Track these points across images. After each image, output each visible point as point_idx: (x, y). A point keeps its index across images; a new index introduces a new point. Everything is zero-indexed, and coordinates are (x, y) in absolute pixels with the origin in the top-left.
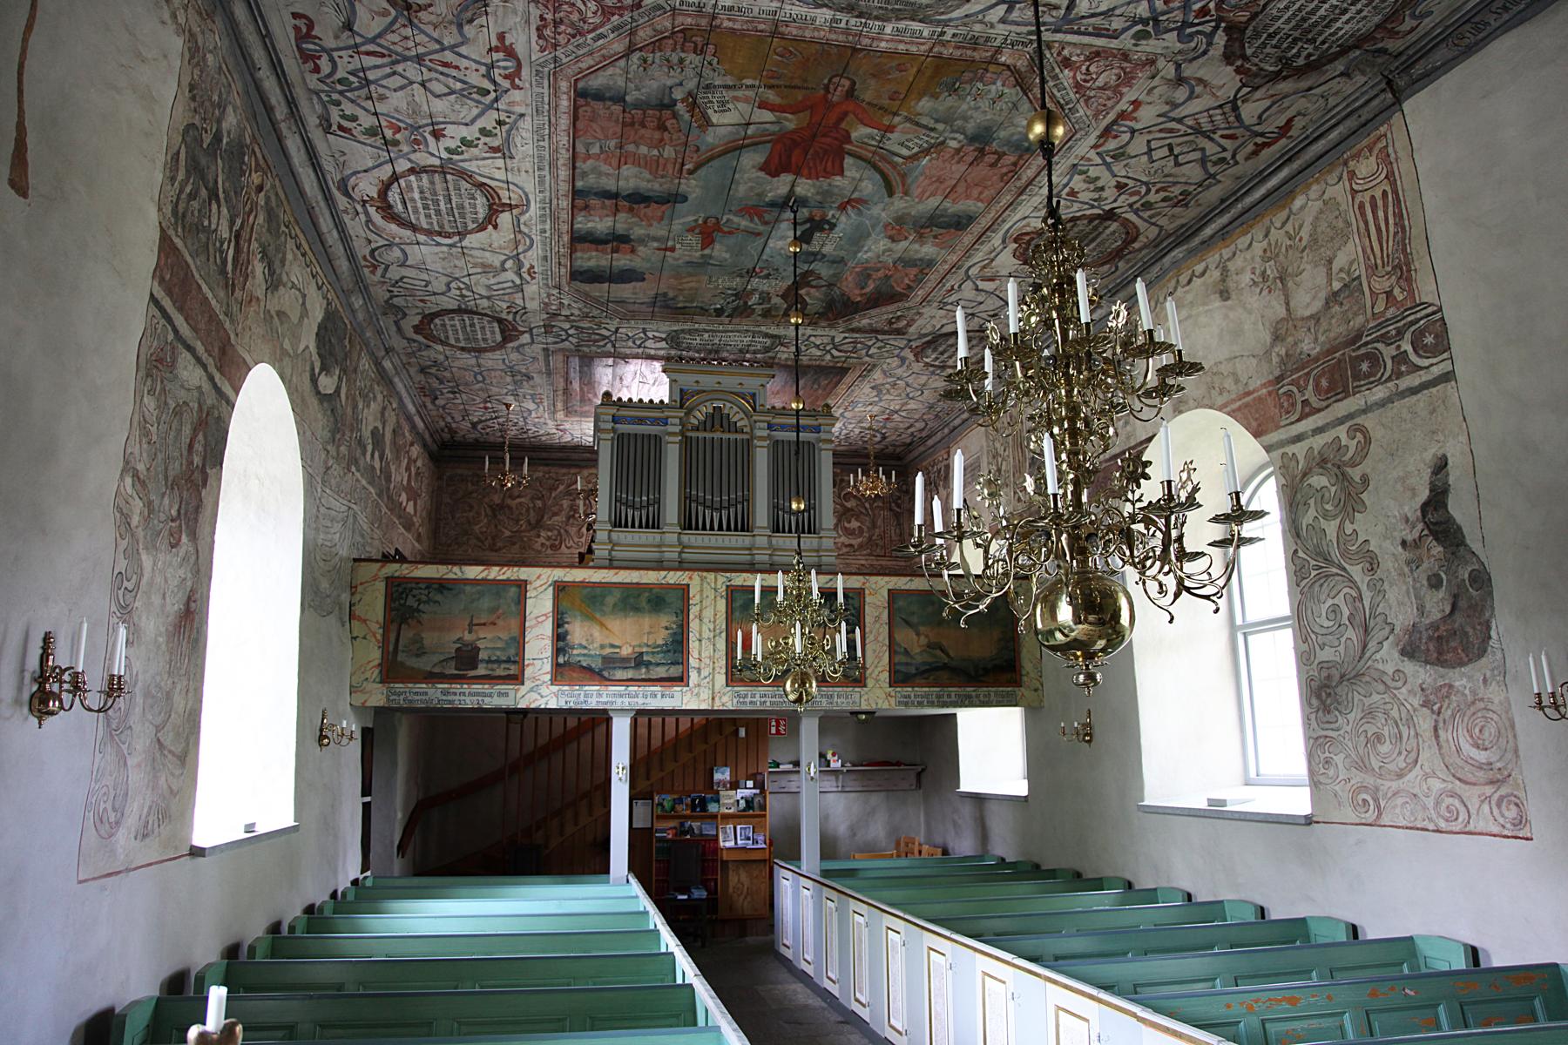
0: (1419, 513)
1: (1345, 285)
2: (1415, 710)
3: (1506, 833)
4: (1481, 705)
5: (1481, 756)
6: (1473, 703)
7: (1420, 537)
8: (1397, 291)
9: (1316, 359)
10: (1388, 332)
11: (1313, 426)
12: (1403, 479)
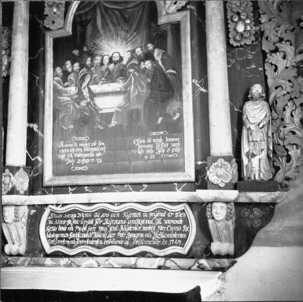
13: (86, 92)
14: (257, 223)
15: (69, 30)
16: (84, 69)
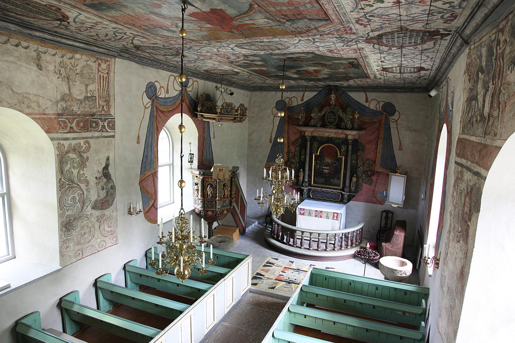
0: (102, 170)
1: (91, 96)
2: (95, 223)
3: (114, 244)
4: (111, 217)
5: (110, 229)
6: (109, 217)
7: (101, 176)
8: (105, 107)
9: (79, 115)
10: (102, 118)
12: (99, 160)
13: (321, 168)
14: (352, 197)
15: (318, 153)
16: (321, 163)
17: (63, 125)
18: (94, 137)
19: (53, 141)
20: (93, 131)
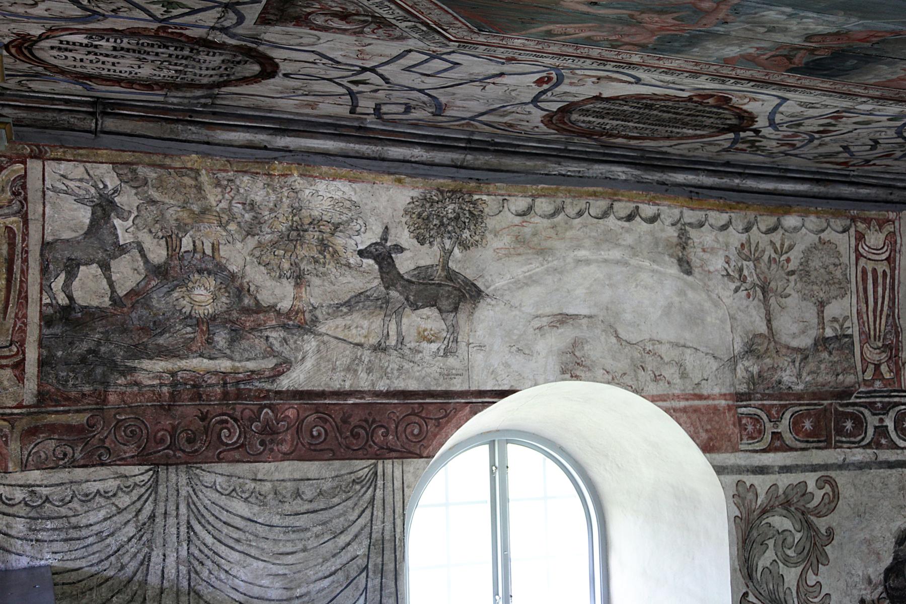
0: (882, 577)
1: (836, 337)
7: (879, 599)
8: (884, 368)
9: (799, 396)
10: (875, 403)
11: (781, 463)
12: (868, 542)
17: (750, 428)
18: (848, 465)
19: (722, 477)
20: (845, 445)
